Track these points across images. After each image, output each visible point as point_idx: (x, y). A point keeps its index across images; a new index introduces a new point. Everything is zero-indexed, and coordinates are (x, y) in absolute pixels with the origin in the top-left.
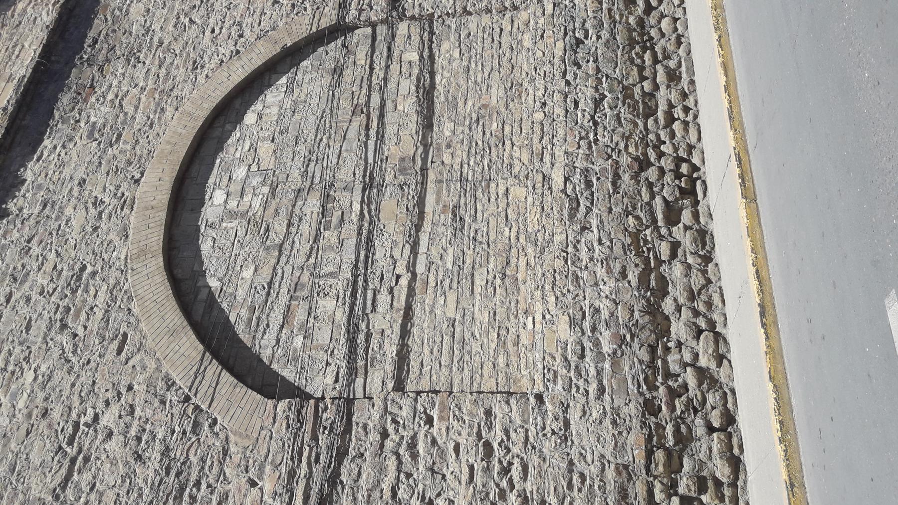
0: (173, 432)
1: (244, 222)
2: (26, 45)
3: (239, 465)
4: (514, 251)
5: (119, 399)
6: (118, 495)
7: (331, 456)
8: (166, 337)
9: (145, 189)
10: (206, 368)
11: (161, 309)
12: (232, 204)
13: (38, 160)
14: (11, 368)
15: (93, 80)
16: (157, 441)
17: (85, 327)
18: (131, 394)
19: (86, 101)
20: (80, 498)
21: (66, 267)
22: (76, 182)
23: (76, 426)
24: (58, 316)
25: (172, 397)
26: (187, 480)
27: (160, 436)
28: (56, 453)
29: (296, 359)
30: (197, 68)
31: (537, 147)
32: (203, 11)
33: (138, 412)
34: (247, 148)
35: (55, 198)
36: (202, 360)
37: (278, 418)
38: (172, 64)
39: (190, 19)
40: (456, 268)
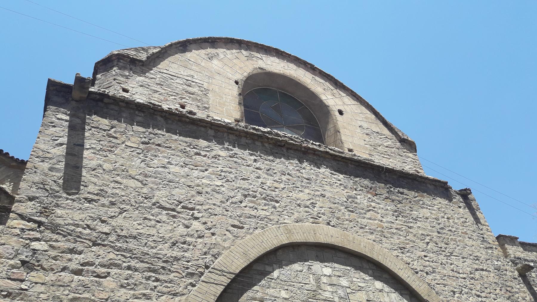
0: (188, 262)
1: (314, 288)
2: (391, 160)
5: (207, 229)
6: (153, 236)
8: (242, 251)
9: (325, 229)
10: (225, 276)
11: (258, 246)
12: (324, 280)
13: (331, 173)
14: (223, 174)
16: (183, 253)
17: (246, 207)
18: (210, 235)
19: (368, 192)
21: (276, 193)
22: (323, 193)
23: (193, 209)
24: (251, 193)
26: (160, 274)
27: (186, 254)
33: (200, 240)
34: (360, 284)
35: (313, 184)
36: (230, 273)
38: (400, 235)
39: (429, 243)
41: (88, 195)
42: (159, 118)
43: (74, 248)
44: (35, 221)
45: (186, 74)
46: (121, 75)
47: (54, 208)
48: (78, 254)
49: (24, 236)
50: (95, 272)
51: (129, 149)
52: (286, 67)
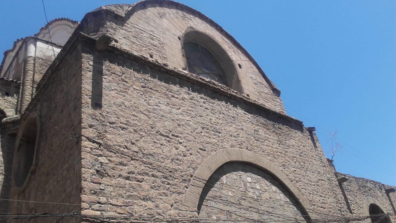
1: (244, 190)
3: (176, 199)
5: (187, 151)
6: (161, 154)
10: (202, 182)
12: (248, 185)
13: (244, 113)
14: (189, 112)
15: (270, 129)
16: (178, 167)
17: (204, 136)
18: (190, 155)
19: (264, 127)
23: (177, 137)
24: (205, 126)
25: (191, 171)
27: (180, 167)
28: (169, 131)
29: (209, 217)
30: (284, 166)
32: (300, 166)
33: (185, 158)
34: (266, 188)
35: (236, 121)
36: (204, 180)
37: (192, 213)
38: (282, 157)
39: (296, 162)
41: (121, 125)
42: (148, 69)
43: (122, 162)
44: (97, 143)
45: (149, 29)
46: (111, 28)
47: (104, 134)
48: (124, 166)
49: (93, 153)
50: (136, 178)
51: (135, 92)
52: (206, 28)
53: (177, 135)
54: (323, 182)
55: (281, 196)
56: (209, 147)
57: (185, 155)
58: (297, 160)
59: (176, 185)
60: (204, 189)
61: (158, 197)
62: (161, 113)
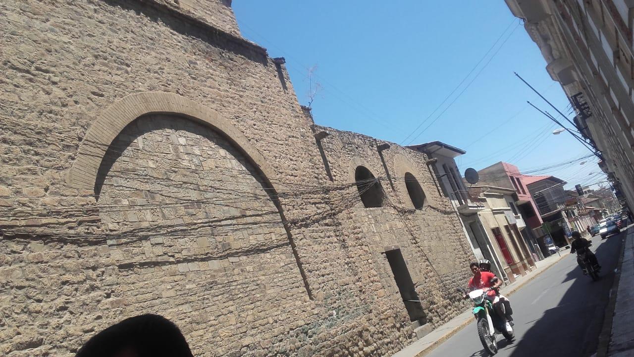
1: (175, 157)
2: (213, 17)
3: (54, 179)
4: (204, 325)
5: (69, 96)
6: (17, 103)
7: (73, 237)
10: (99, 148)
12: (181, 149)
13: (171, 33)
14: (67, 27)
15: (215, 60)
16: (53, 124)
17: (99, 71)
18: (74, 103)
19: (205, 57)
20: (8, 79)
21: (126, 55)
22: (168, 56)
23: (47, 71)
24: (101, 53)
25: (79, 130)
28: (28, 60)
29: (116, 202)
30: (237, 119)
31: (257, 323)
32: (261, 118)
34: (209, 152)
35: (157, 45)
38: (235, 104)
40: (187, 291)
53: (46, 68)
54: (294, 139)
55: (234, 164)
56: (109, 90)
57: (65, 104)
58: (257, 109)
59: (51, 155)
60: (104, 160)
61: (18, 176)
62: (11, 27)
